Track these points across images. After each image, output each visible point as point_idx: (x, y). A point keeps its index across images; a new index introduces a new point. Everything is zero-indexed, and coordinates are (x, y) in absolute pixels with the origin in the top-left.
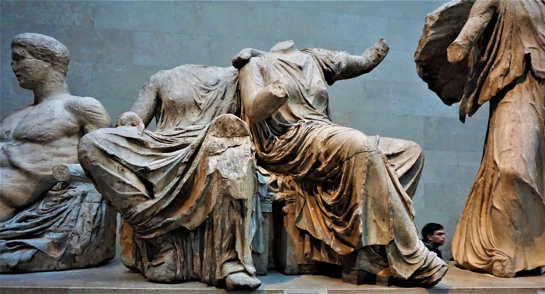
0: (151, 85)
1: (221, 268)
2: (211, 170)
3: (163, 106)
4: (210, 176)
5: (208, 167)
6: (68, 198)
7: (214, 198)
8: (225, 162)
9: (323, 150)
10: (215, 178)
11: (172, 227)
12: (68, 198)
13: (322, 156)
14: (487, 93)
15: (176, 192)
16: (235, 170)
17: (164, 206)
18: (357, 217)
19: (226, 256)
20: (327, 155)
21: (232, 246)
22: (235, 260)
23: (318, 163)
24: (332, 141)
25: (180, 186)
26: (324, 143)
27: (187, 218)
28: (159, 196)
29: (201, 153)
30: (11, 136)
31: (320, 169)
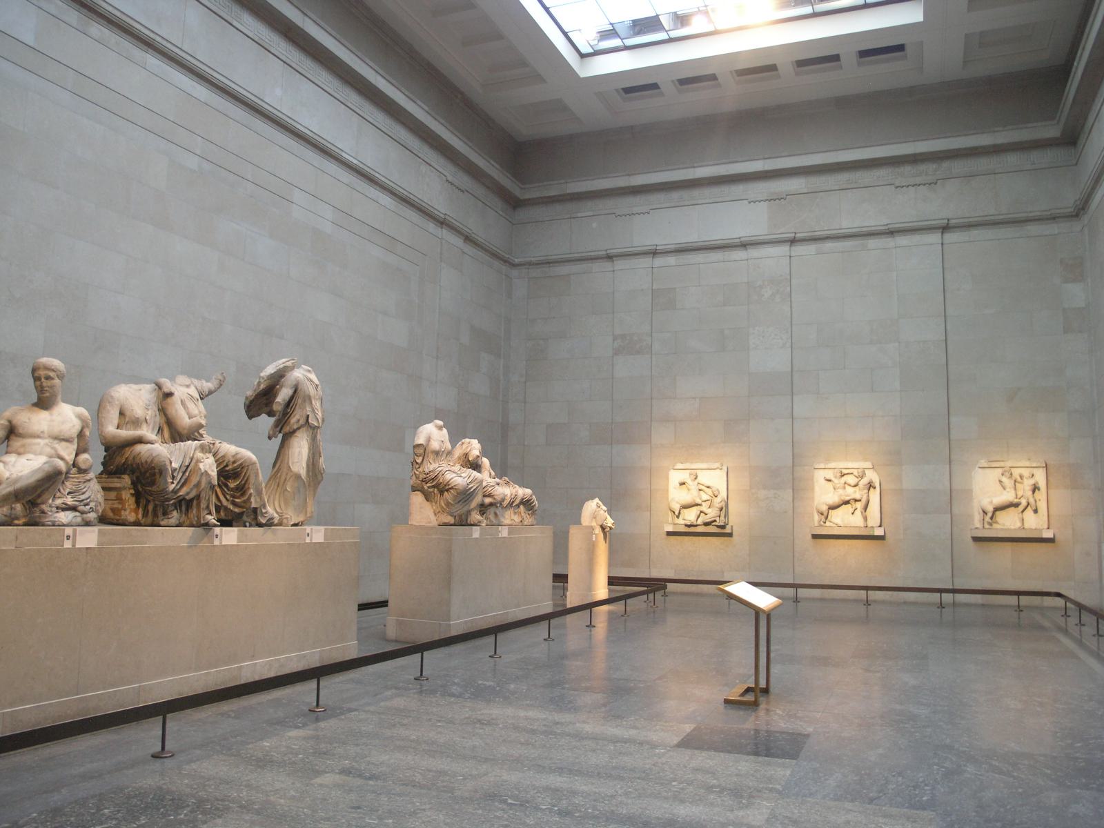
0: (117, 403)
1: (204, 517)
2: (203, 471)
3: (127, 420)
4: (202, 474)
5: (200, 469)
6: (89, 480)
7: (203, 485)
8: (208, 466)
9: (232, 460)
10: (204, 475)
11: (181, 498)
12: (89, 480)
13: (231, 463)
14: (287, 429)
15: (183, 480)
16: (213, 471)
17: (178, 487)
18: (251, 494)
19: (206, 512)
20: (234, 462)
21: (208, 507)
22: (210, 513)
23: (227, 466)
24: (238, 456)
25: (184, 477)
26: (233, 456)
27: (188, 494)
28: (175, 482)
29: (194, 461)
30: (46, 435)
31: (227, 469)
